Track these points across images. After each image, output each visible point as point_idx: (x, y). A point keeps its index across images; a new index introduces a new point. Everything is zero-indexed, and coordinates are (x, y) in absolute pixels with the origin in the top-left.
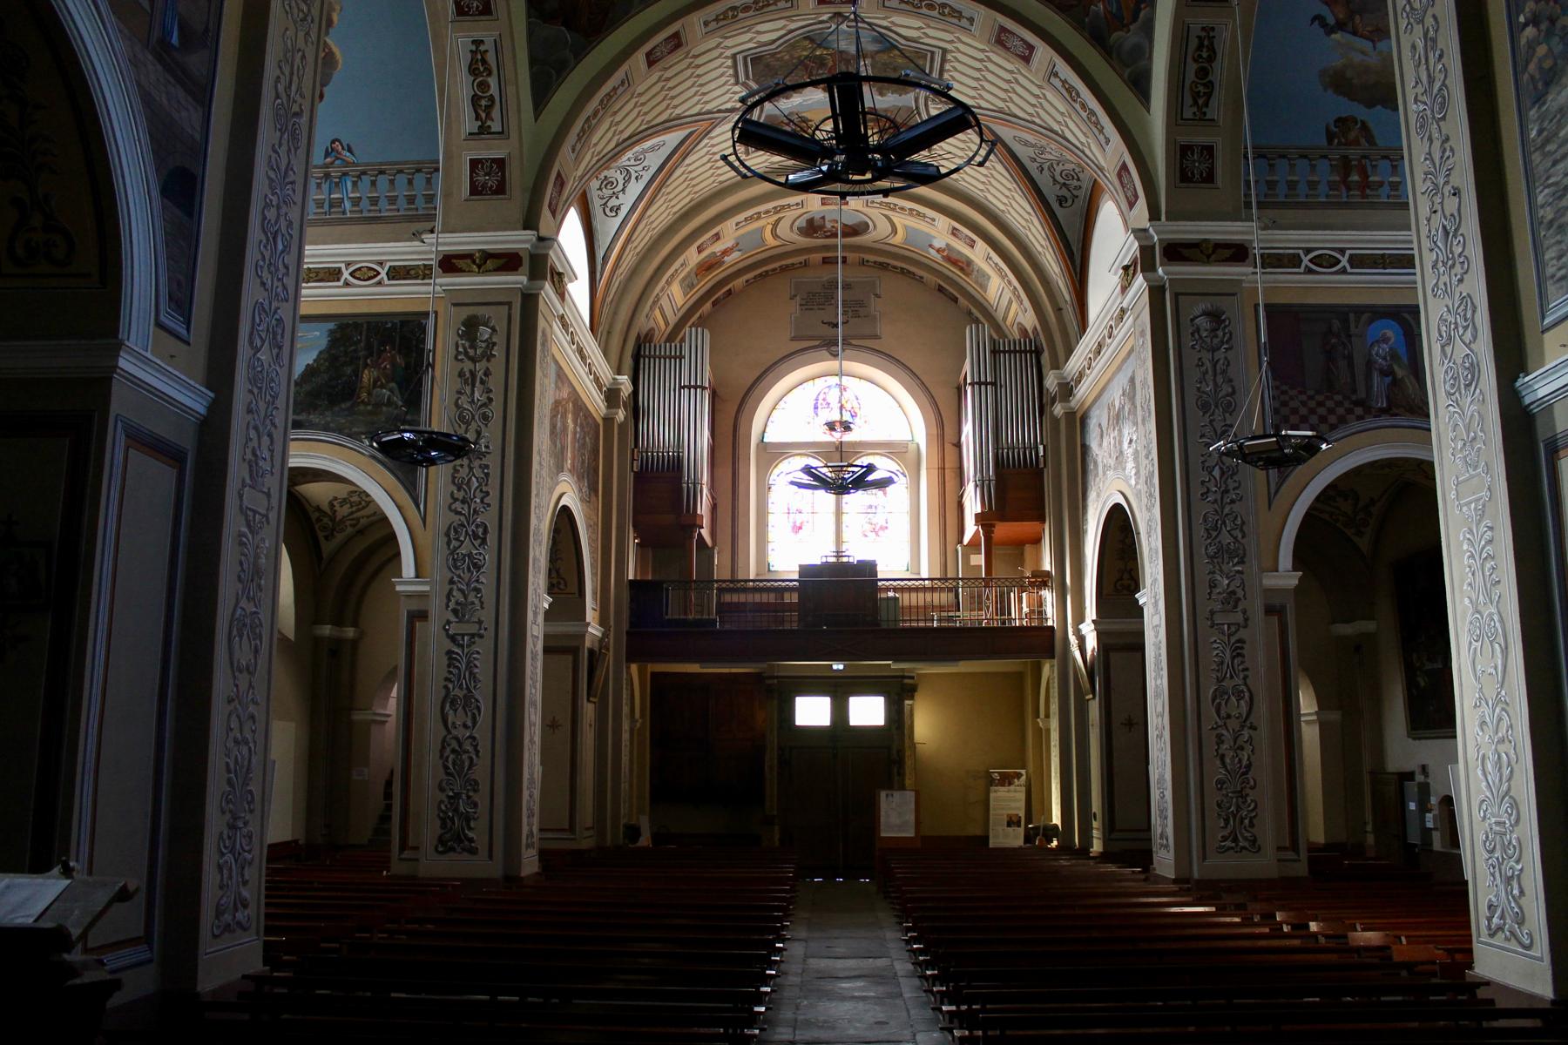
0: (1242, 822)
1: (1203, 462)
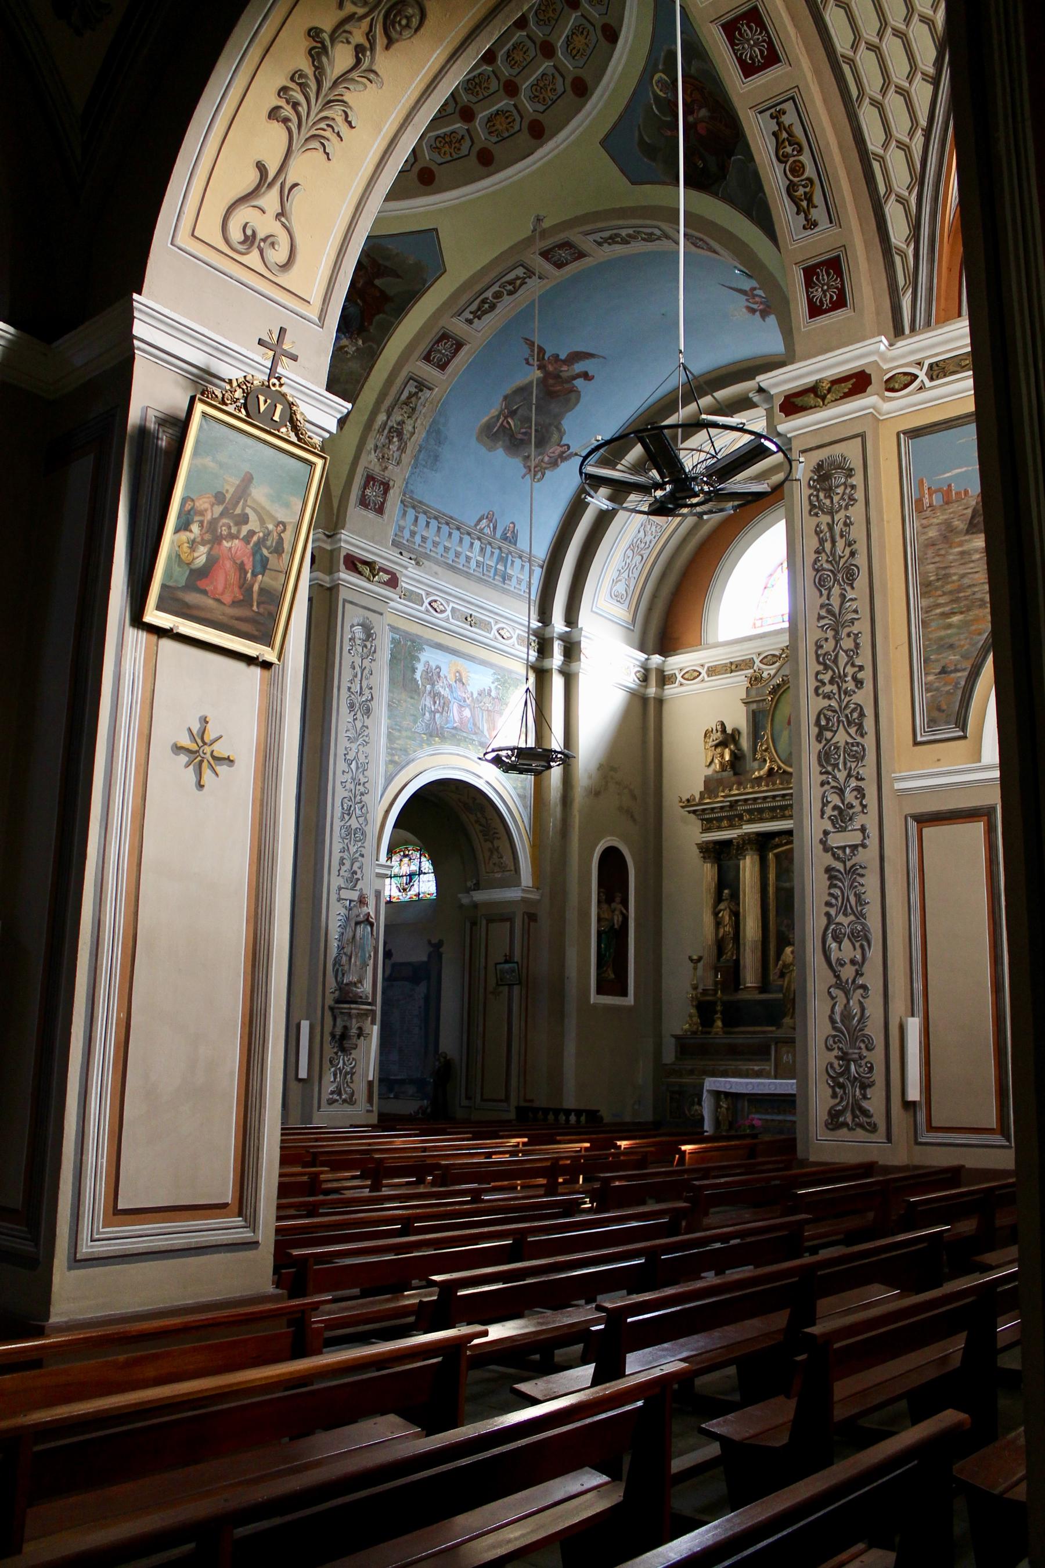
0: (345, 1078)
1: (345, 755)
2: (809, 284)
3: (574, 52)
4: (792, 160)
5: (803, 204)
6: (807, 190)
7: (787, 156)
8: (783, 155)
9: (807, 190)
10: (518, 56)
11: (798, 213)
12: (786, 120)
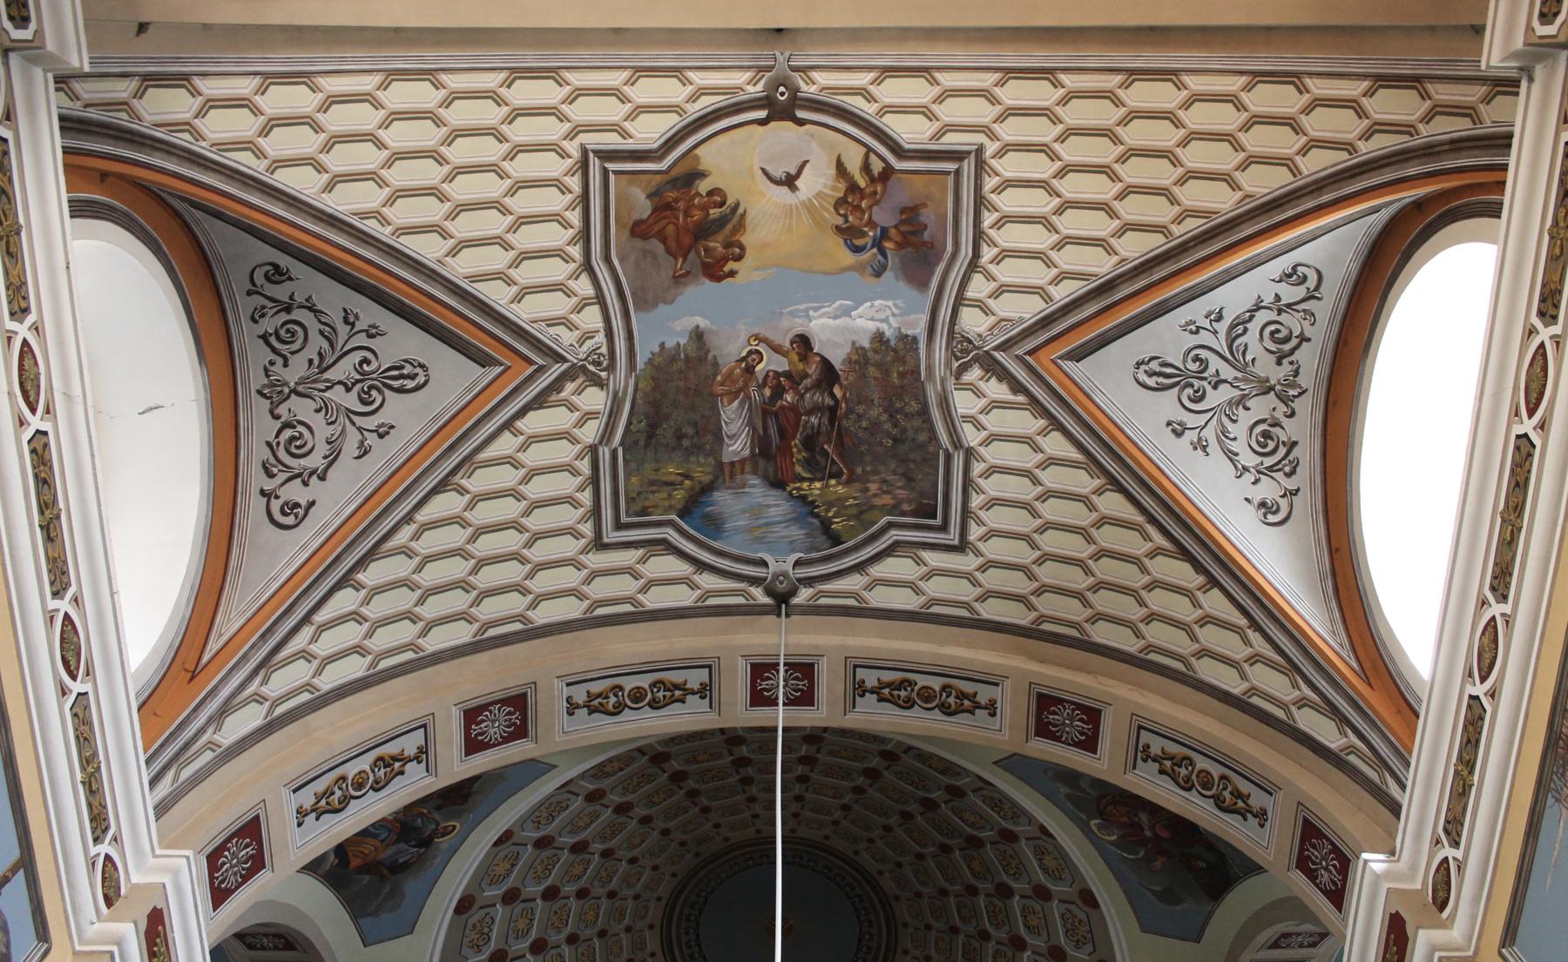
2: (1312, 876)
3: (1056, 873)
4: (1194, 777)
5: (1236, 805)
6: (1230, 788)
7: (1188, 779)
8: (1185, 783)
9: (1230, 788)
10: (1033, 922)
11: (1245, 819)
12: (1155, 750)
